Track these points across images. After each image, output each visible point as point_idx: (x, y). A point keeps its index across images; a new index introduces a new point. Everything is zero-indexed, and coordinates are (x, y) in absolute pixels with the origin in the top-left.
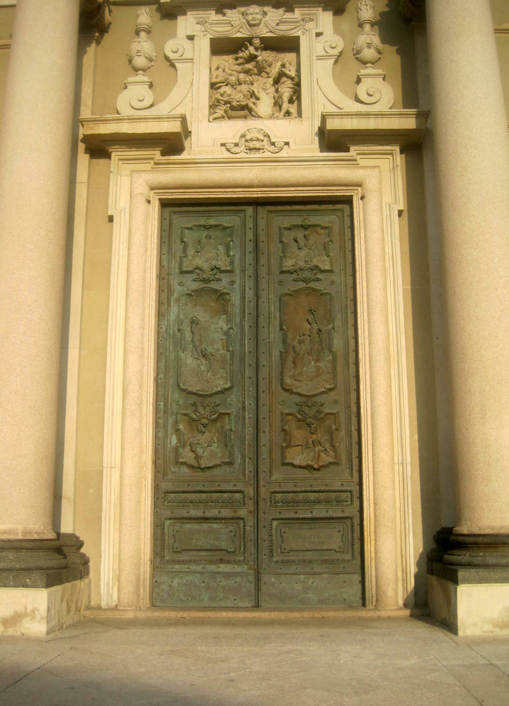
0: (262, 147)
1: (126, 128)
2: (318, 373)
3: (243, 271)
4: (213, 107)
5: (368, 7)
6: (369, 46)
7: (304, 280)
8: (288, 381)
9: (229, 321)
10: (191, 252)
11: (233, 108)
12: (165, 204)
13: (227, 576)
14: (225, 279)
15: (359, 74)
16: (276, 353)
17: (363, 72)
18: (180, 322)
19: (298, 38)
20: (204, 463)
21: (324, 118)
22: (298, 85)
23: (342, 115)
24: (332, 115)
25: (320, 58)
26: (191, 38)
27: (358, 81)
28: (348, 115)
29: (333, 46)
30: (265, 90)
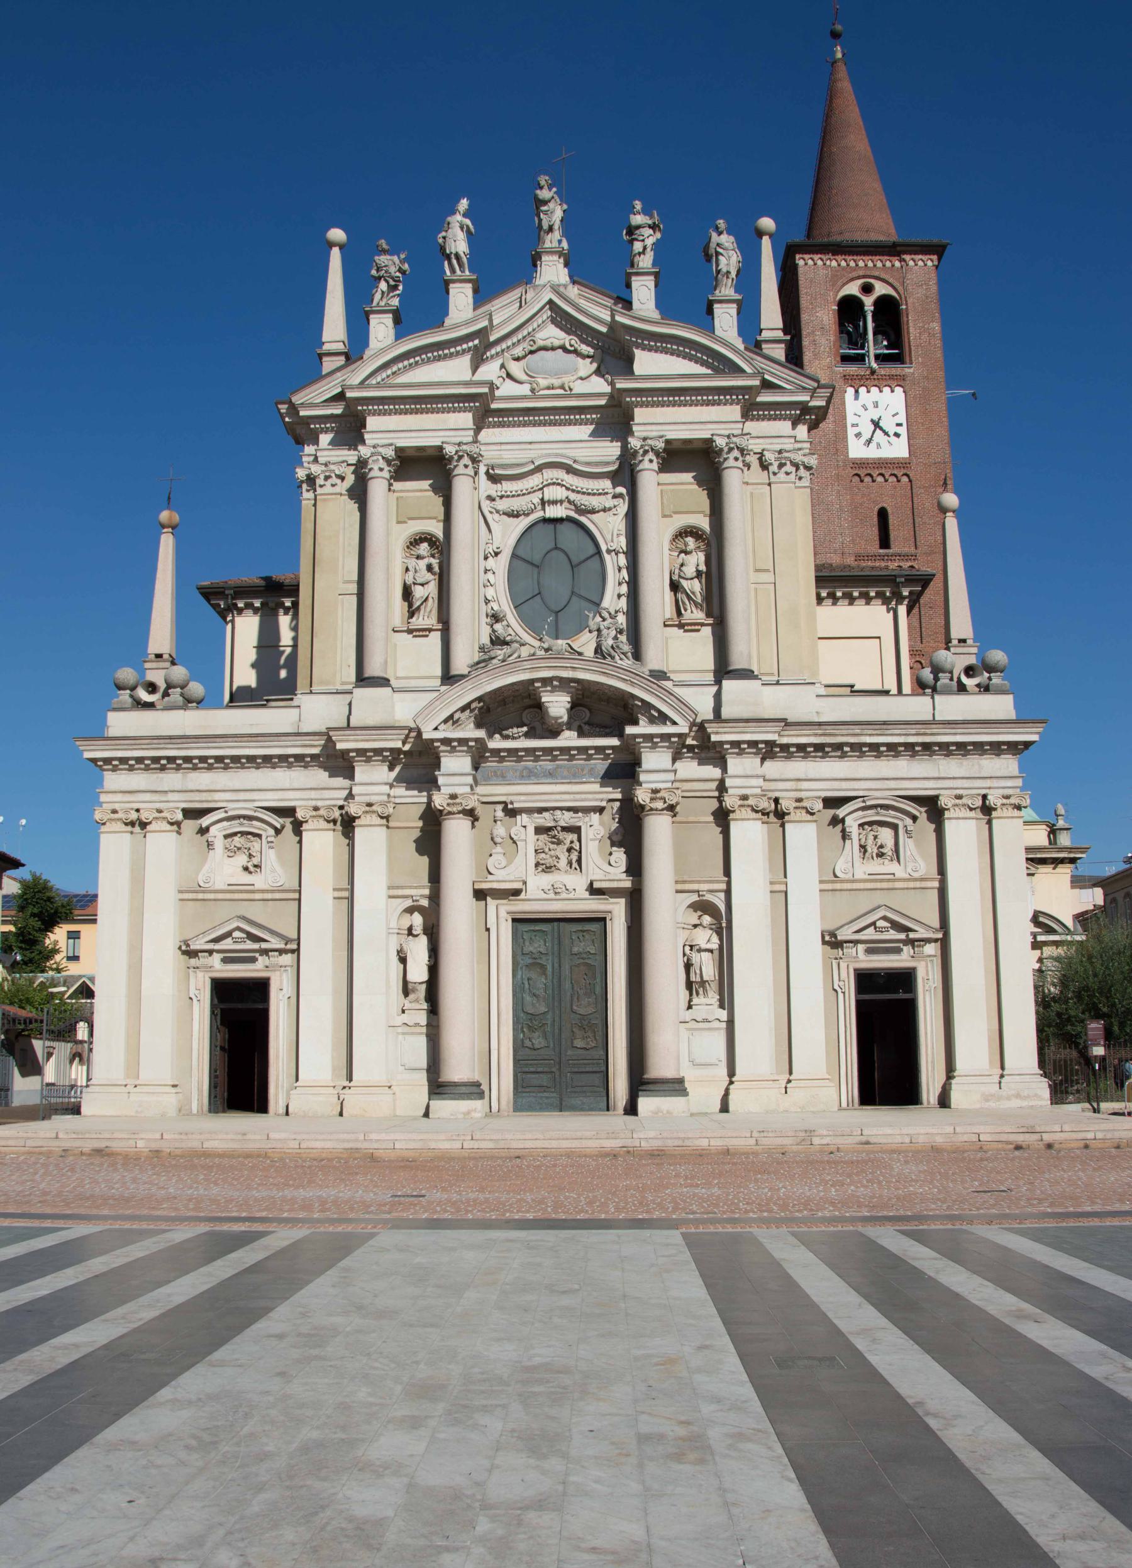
1: (495, 886)
2: (589, 1004)
3: (553, 954)
4: (537, 865)
7: (583, 958)
8: (575, 1008)
9: (546, 979)
10: (527, 943)
11: (547, 868)
12: (514, 920)
13: (547, 1098)
14: (544, 958)
16: (569, 994)
18: (522, 978)
20: (536, 1046)
25: (591, 840)
26: (525, 827)
27: (611, 854)
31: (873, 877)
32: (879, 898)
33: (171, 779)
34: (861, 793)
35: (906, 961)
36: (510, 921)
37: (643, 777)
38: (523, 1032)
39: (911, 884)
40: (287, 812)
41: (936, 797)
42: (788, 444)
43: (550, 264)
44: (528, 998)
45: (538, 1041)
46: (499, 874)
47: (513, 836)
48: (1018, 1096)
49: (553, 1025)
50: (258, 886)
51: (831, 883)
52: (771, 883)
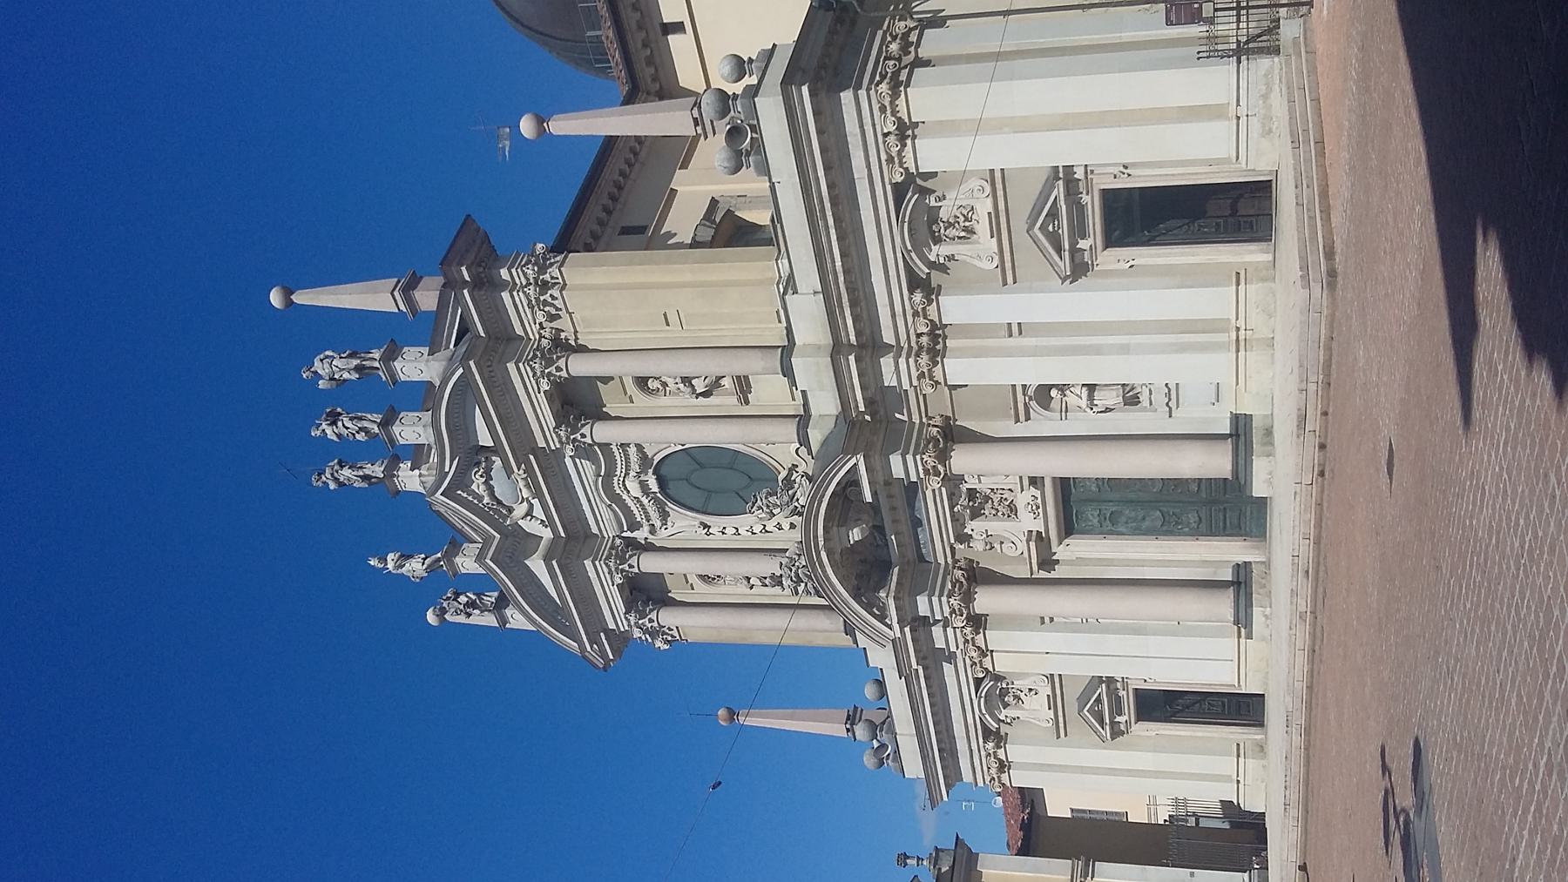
31: (995, 232)
32: (1019, 224)
33: (961, 745)
34: (899, 255)
35: (1092, 197)
36: (1067, 541)
37: (914, 478)
38: (1182, 529)
39: (1000, 193)
40: (978, 682)
41: (895, 186)
42: (520, 297)
43: (403, 485)
44: (1147, 524)
45: (1192, 518)
46: (1022, 546)
48: (1265, 97)
49: (1174, 507)
50: (1050, 693)
51: (1007, 275)
52: (1011, 336)
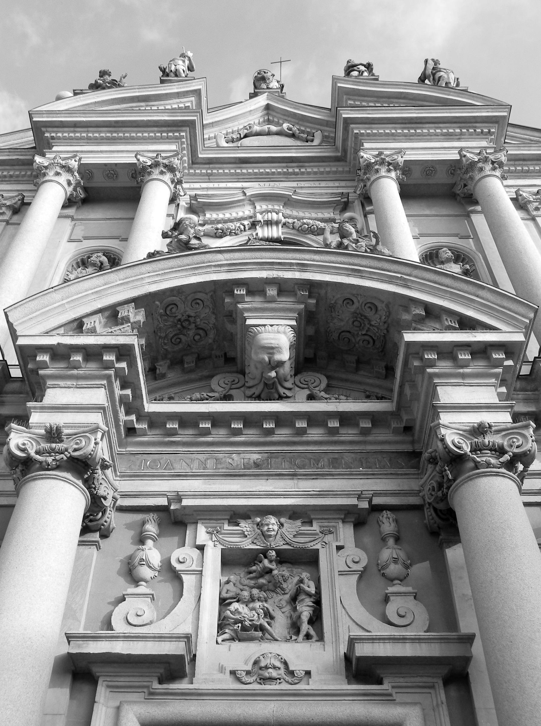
0: (278, 677)
5: (391, 520)
6: (396, 561)
15: (387, 591)
17: (391, 589)
19: (318, 550)
21: (352, 642)
22: (318, 603)
23: (373, 639)
24: (361, 640)
25: (342, 573)
26: (201, 548)
27: (386, 599)
28: (379, 639)
29: (356, 560)
30: (280, 608)
47: (174, 563)
